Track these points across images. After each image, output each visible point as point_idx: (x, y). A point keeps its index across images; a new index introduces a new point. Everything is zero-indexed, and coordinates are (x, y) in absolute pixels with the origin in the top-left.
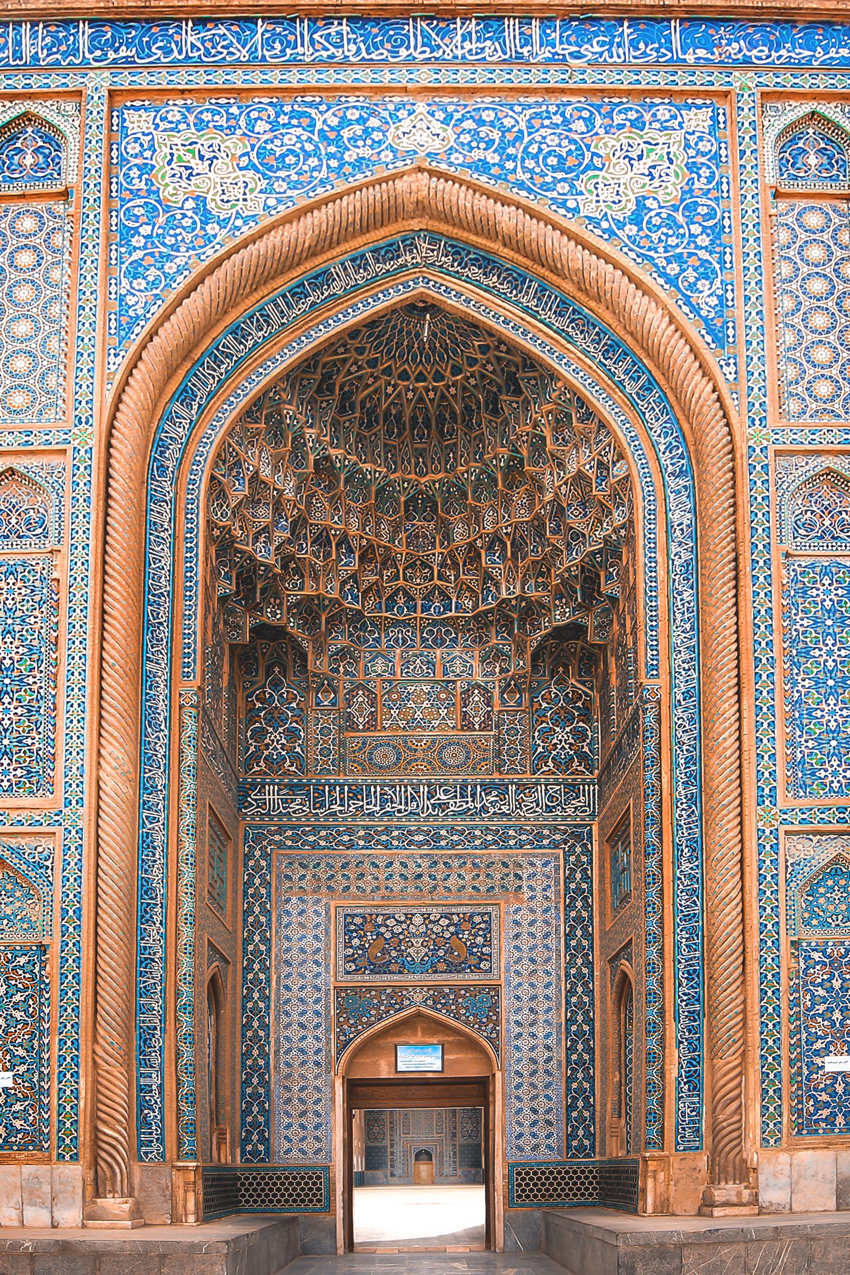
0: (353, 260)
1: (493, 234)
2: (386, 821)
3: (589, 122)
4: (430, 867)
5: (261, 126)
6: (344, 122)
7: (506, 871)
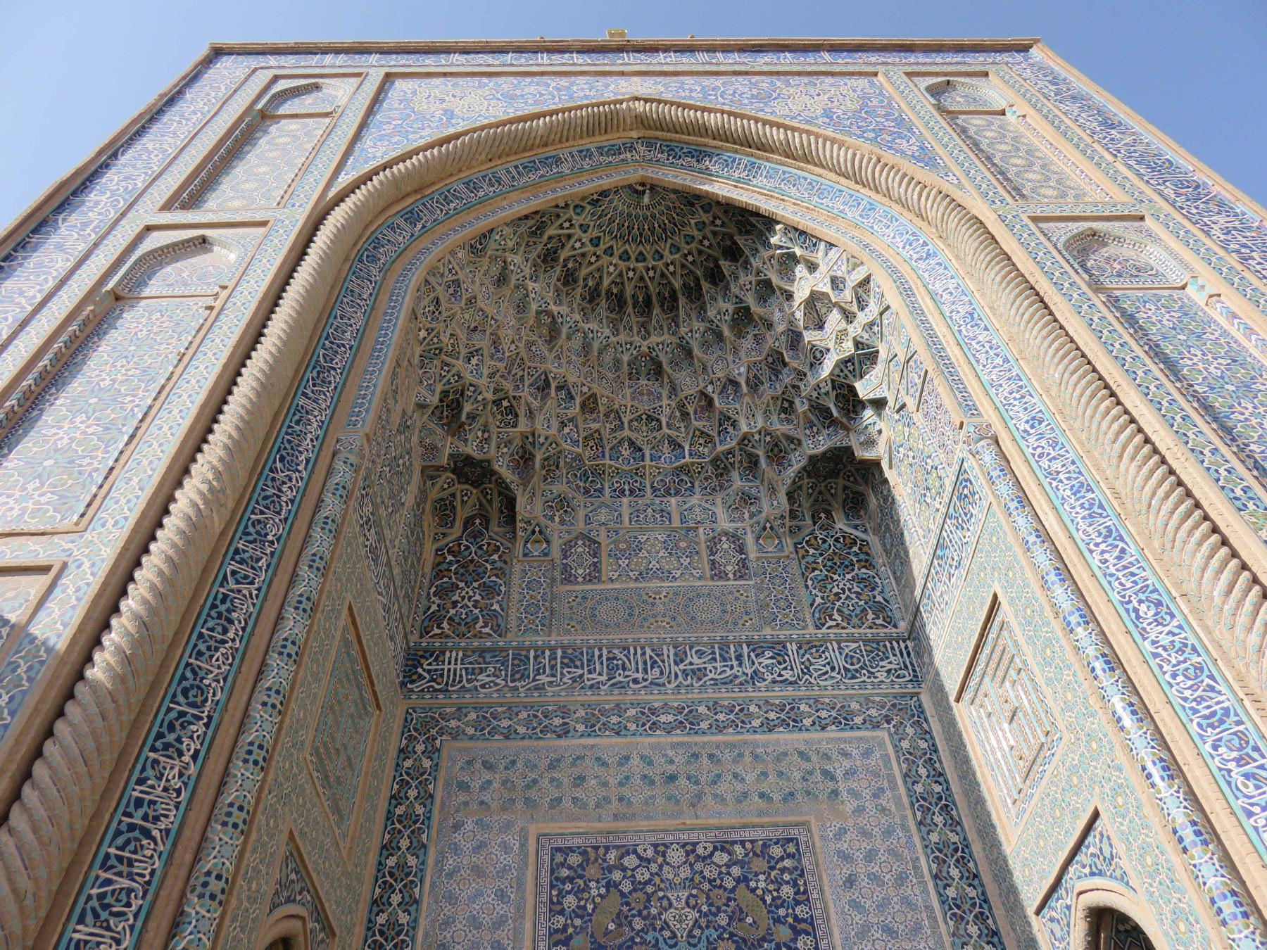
0: (580, 151)
1: (703, 131)
2: (616, 697)
4: (689, 762)
7: (808, 766)
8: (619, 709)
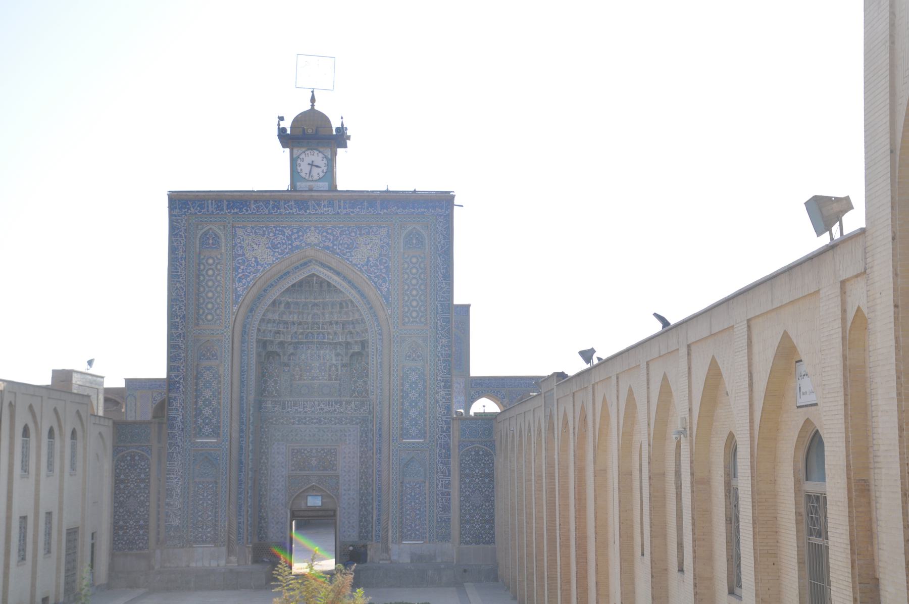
3: (356, 233)
5: (271, 234)
6: (293, 233)
8: (305, 418)
